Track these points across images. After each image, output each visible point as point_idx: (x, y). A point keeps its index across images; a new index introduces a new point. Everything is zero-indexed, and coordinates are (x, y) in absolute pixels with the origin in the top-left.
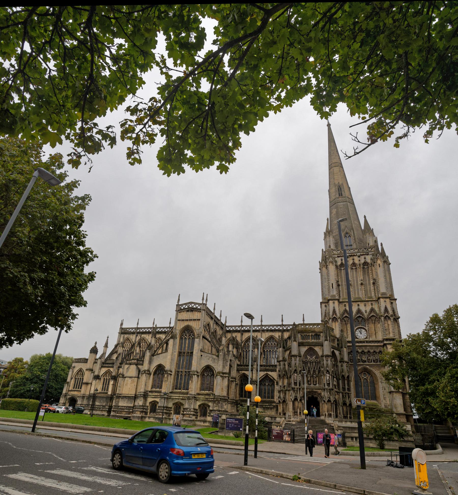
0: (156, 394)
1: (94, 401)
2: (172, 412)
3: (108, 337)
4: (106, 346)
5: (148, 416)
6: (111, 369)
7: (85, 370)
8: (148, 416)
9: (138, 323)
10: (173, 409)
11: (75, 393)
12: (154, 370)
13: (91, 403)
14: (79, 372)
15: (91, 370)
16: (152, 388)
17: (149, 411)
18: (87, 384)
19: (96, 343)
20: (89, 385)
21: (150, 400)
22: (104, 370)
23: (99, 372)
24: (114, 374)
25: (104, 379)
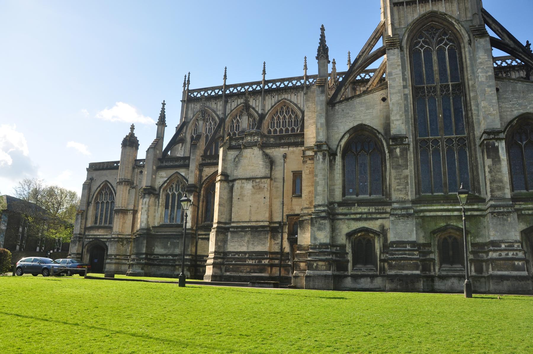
0: (365, 209)
1: (150, 246)
2: (432, 256)
3: (164, 104)
4: (162, 122)
5: (350, 272)
6: (183, 172)
7: (114, 185)
8: (350, 272)
9: (225, 76)
10: (434, 248)
11: (99, 233)
12: (343, 143)
13: (144, 251)
14: (102, 189)
15: (129, 183)
16: (344, 195)
17: (350, 257)
18: (124, 212)
19: (132, 128)
20: (130, 216)
21: (345, 228)
22: (163, 177)
23: (153, 180)
24: (192, 180)
25: (167, 196)
